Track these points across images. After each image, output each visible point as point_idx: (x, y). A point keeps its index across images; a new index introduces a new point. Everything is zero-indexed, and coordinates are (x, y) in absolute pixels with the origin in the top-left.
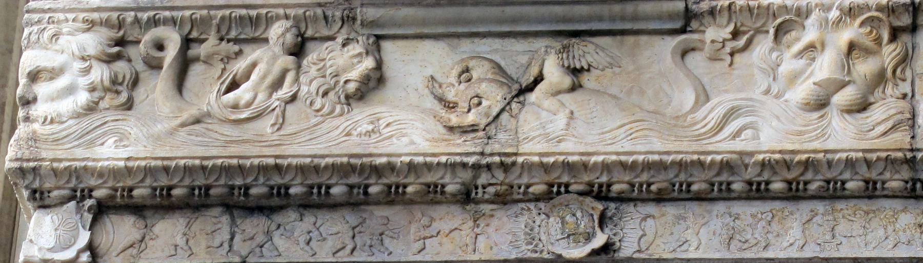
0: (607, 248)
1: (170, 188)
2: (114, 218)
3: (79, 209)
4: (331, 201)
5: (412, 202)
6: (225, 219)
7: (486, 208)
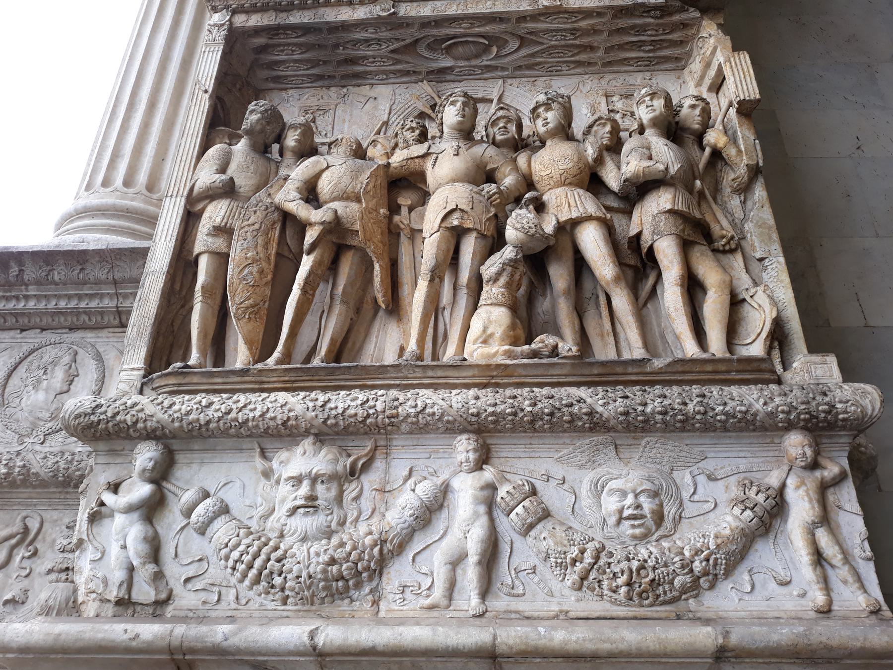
0: (394, 13)
1: (256, 4)
2: (239, 15)
3: (227, 12)
4: (307, 6)
5: (333, 6)
6: (274, 13)
7: (357, 6)
